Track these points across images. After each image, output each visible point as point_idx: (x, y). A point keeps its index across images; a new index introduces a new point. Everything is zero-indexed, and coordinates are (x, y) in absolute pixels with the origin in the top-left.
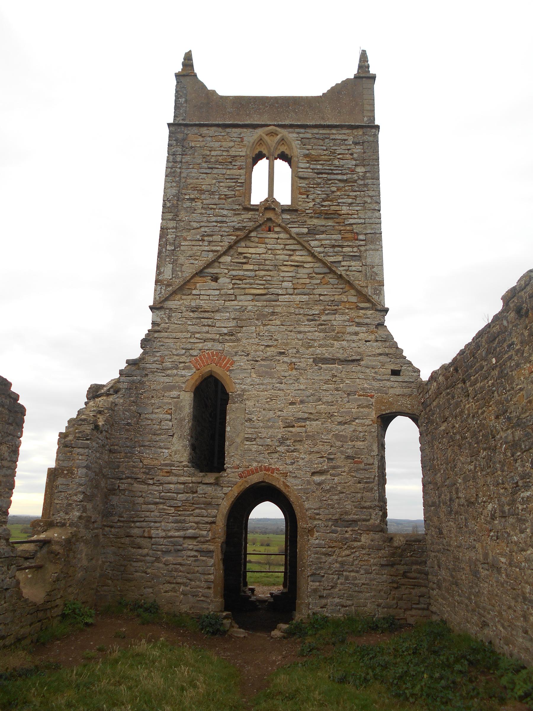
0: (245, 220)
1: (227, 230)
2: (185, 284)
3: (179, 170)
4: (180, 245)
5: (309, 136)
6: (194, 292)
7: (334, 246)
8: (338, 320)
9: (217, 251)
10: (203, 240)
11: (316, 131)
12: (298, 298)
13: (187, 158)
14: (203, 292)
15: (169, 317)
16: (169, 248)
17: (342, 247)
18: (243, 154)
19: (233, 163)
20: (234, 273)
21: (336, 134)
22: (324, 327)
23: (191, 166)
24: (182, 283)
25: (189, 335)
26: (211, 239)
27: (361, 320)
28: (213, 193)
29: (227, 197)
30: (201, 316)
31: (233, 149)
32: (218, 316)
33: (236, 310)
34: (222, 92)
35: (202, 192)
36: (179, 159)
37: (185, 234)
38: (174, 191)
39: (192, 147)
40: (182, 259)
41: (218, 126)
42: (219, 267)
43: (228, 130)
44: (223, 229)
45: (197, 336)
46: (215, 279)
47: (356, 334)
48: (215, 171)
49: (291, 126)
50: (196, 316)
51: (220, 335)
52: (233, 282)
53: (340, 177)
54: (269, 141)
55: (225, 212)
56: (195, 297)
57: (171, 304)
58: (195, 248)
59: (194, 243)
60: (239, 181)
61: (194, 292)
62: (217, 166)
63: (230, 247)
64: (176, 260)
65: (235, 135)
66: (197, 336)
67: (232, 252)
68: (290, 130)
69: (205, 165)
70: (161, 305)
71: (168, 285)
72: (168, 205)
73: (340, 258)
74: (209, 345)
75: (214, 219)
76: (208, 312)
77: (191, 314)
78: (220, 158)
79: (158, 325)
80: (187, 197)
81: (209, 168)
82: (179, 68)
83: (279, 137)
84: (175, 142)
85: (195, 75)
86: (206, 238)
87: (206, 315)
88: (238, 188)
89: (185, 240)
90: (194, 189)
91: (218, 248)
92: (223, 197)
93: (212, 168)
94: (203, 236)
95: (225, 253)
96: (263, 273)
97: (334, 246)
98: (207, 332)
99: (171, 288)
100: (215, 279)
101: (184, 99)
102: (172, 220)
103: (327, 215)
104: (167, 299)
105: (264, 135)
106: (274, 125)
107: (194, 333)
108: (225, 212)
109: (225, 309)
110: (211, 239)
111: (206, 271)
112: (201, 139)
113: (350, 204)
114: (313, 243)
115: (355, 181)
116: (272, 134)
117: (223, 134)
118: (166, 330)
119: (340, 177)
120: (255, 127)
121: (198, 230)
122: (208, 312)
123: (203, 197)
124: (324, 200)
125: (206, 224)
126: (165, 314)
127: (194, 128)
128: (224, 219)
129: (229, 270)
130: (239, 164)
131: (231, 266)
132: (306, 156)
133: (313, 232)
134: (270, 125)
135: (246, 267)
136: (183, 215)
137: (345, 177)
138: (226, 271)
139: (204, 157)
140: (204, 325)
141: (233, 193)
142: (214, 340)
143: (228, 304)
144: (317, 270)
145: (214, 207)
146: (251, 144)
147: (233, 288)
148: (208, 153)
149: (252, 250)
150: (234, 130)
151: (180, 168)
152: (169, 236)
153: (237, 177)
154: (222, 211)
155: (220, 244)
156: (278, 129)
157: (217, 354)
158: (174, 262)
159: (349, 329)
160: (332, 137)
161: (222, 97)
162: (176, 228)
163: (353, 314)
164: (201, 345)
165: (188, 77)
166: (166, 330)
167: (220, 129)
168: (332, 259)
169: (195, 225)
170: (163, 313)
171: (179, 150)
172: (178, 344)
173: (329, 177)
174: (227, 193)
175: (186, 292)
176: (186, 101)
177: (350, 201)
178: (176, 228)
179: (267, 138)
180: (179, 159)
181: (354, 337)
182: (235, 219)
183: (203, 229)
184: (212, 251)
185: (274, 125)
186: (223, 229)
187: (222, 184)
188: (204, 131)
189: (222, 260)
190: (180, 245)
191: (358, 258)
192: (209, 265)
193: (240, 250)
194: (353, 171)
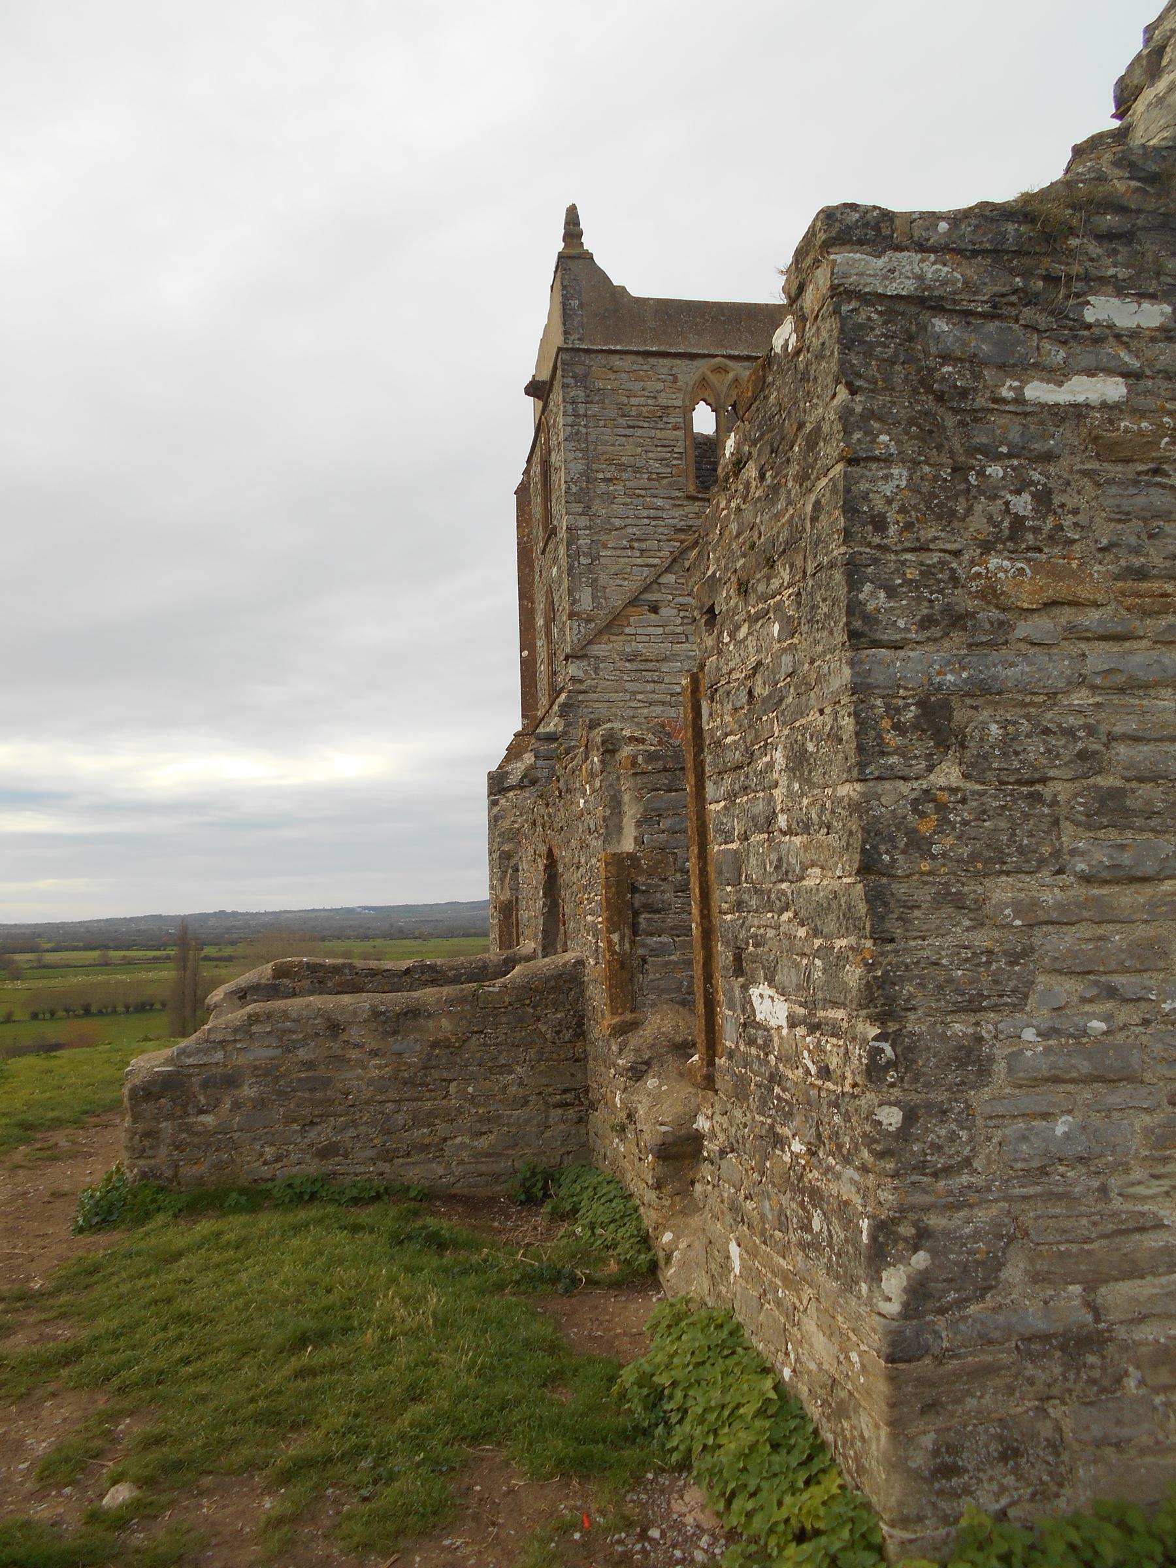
0: (690, 516)
1: (666, 532)
2: (614, 619)
3: (584, 431)
4: (599, 557)
6: (627, 630)
9: (655, 566)
10: (632, 548)
13: (595, 409)
14: (640, 631)
15: (596, 670)
16: (583, 560)
18: (680, 403)
19: (665, 419)
20: (681, 600)
23: (601, 423)
24: (610, 618)
25: (628, 696)
26: (643, 546)
28: (637, 470)
29: (660, 477)
30: (642, 667)
31: (663, 394)
32: (665, 667)
33: (689, 657)
34: (637, 290)
35: (622, 467)
36: (582, 412)
37: (603, 538)
39: (599, 389)
40: (603, 579)
41: (637, 353)
42: (660, 591)
43: (653, 361)
44: (660, 530)
45: (640, 697)
46: (654, 609)
48: (640, 432)
50: (635, 668)
51: (672, 695)
52: (682, 614)
54: (718, 385)
55: (660, 503)
56: (629, 638)
58: (622, 560)
59: (619, 552)
60: (676, 450)
61: (627, 630)
62: (641, 424)
63: (674, 560)
64: (596, 580)
65: (665, 370)
66: (640, 697)
67: (676, 567)
68: (746, 364)
69: (622, 421)
70: (583, 652)
71: (588, 621)
72: (574, 489)
74: (658, 710)
75: (645, 513)
76: (651, 661)
77: (627, 664)
78: (644, 409)
79: (581, 681)
80: (601, 476)
81: (629, 427)
83: (731, 376)
84: (572, 381)
85: (589, 257)
86: (636, 545)
87: (650, 665)
88: (675, 462)
89: (605, 547)
90: (610, 462)
91: (656, 561)
92: (654, 476)
93: (633, 427)
94: (632, 540)
95: (668, 570)
98: (653, 692)
99: (593, 625)
100: (654, 609)
101: (577, 302)
102: (583, 514)
104: (590, 642)
105: (709, 373)
106: (723, 356)
107: (634, 693)
108: (660, 503)
109: (674, 657)
110: (643, 546)
111: (642, 597)
112: (612, 376)
116: (721, 370)
117: (645, 367)
118: (593, 689)
120: (693, 357)
121: (623, 531)
122: (651, 661)
123: (625, 476)
125: (634, 522)
126: (589, 665)
127: (600, 356)
128: (660, 514)
129: (674, 596)
130: (673, 420)
131: (676, 589)
134: (717, 356)
136: (597, 507)
138: (671, 597)
140: (648, 681)
141: (669, 470)
142: (663, 703)
143: (677, 647)
145: (643, 492)
146: (690, 388)
147: (681, 624)
148: (626, 400)
150: (662, 361)
151: (585, 426)
152: (581, 542)
153: (672, 443)
154: (655, 500)
155: (658, 554)
156: (728, 362)
157: (670, 724)
158: (594, 584)
161: (638, 300)
162: (590, 528)
164: (646, 711)
165: (581, 261)
166: (593, 689)
167: (640, 359)
169: (617, 522)
170: (586, 663)
171: (580, 393)
172: (614, 710)
174: (660, 471)
175: (616, 630)
176: (581, 305)
178: (590, 528)
179: (712, 378)
180: (582, 412)
182: (677, 512)
183: (630, 530)
184: (647, 566)
185: (723, 356)
186: (660, 530)
187: (651, 455)
188: (616, 361)
189: (661, 580)
190: (599, 557)
192: (647, 589)
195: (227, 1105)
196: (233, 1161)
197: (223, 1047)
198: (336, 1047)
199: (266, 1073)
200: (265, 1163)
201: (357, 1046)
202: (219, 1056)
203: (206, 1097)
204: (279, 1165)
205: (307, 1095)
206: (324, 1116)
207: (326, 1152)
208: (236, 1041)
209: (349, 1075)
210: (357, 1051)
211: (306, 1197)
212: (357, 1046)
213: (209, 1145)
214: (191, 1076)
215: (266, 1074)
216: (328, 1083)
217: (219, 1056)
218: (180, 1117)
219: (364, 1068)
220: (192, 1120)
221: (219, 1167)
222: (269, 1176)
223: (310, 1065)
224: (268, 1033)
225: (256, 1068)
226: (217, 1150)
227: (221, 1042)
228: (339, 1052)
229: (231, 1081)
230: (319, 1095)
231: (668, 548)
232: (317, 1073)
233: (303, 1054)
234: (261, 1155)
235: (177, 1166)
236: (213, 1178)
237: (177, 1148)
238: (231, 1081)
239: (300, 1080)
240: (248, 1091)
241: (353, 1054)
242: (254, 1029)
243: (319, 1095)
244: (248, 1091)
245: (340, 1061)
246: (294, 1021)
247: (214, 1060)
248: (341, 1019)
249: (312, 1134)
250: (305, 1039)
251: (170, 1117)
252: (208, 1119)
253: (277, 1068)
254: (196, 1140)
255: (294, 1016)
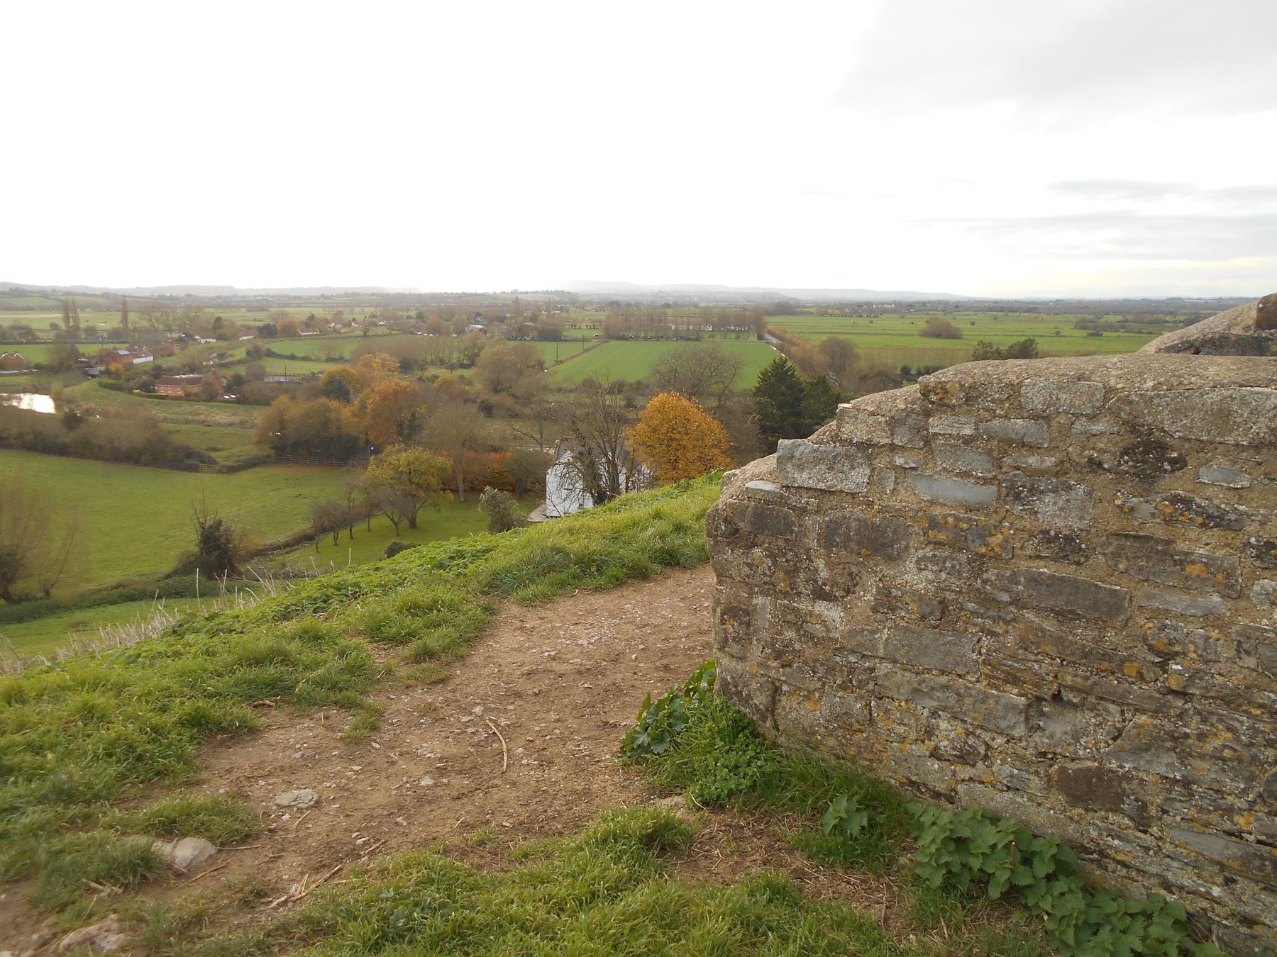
195: (867, 595)
196: (871, 721)
197: (869, 458)
198: (1148, 513)
199: (959, 539)
200: (935, 754)
201: (1214, 520)
202: (857, 478)
203: (830, 566)
204: (965, 772)
205: (1050, 625)
206: (1091, 698)
207: (1089, 789)
208: (893, 448)
209: (1178, 602)
210: (1214, 535)
211: (995, 892)
212: (1214, 520)
213: (831, 670)
214: (804, 511)
215: (957, 544)
216: (1109, 608)
217: (857, 478)
218: (786, 595)
219: (1232, 592)
220: (804, 605)
221: (844, 723)
222: (941, 787)
223: (1066, 546)
224: (968, 441)
225: (934, 524)
226: (843, 687)
227: (863, 446)
228: (1157, 530)
229: (880, 542)
230: (1083, 634)
232: (1083, 575)
233: (1052, 511)
234: (929, 732)
235: (776, 690)
236: (832, 742)
237: (778, 655)
238: (880, 542)
239: (1035, 580)
240: (914, 577)
241: (1200, 545)
242: (937, 424)
243: (1083, 634)
244: (914, 577)
245: (1158, 555)
246: (1035, 417)
247: (849, 486)
248: (1175, 429)
249: (1059, 727)
250: (1060, 470)
251: (769, 588)
252: (832, 613)
253: (984, 534)
254: (810, 652)
255: (1037, 403)
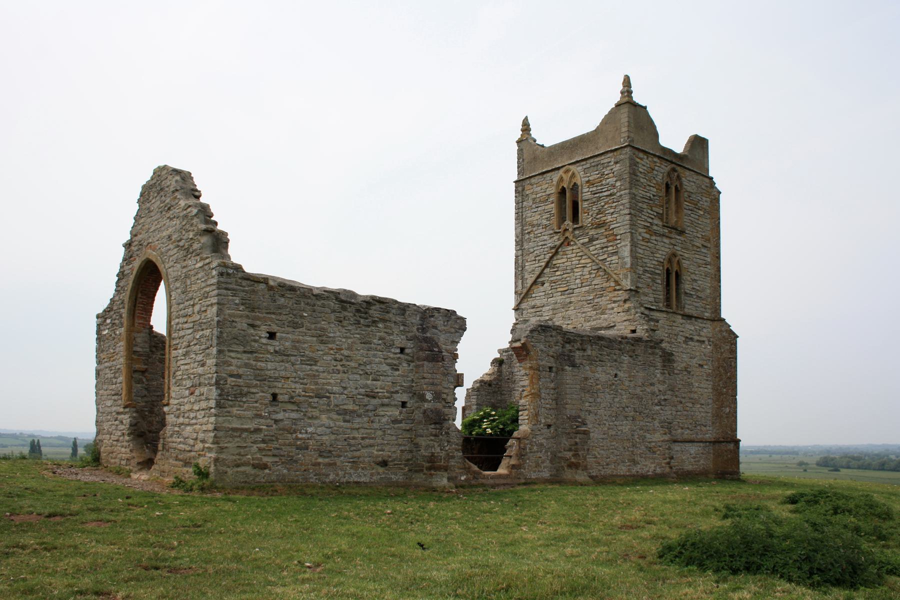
5: (588, 165)
7: (602, 248)
8: (603, 301)
11: (592, 160)
12: (584, 289)
13: (525, 203)
17: (607, 247)
20: (552, 279)
21: (604, 160)
22: (595, 307)
27: (615, 299)
29: (546, 226)
35: (533, 226)
38: (519, 230)
47: (613, 308)
49: (577, 162)
53: (605, 194)
55: (545, 237)
57: (523, 306)
73: (606, 256)
82: (518, 134)
96: (565, 276)
97: (602, 248)
100: (543, 284)
103: (599, 226)
108: (545, 237)
113: (612, 213)
114: (591, 248)
115: (615, 194)
116: (567, 171)
119: (605, 194)
120: (558, 169)
124: (598, 214)
132: (588, 182)
133: (591, 240)
135: (558, 273)
136: (526, 246)
137: (608, 193)
139: (534, 199)
144: (594, 268)
149: (559, 261)
156: (571, 167)
159: (609, 306)
160: (602, 162)
163: (611, 295)
167: (540, 177)
168: (601, 258)
169: (532, 250)
173: (601, 195)
177: (612, 210)
181: (612, 311)
188: (533, 180)
191: (616, 253)
192: (538, 277)
193: (554, 262)
194: (614, 186)
231: (548, 256)
